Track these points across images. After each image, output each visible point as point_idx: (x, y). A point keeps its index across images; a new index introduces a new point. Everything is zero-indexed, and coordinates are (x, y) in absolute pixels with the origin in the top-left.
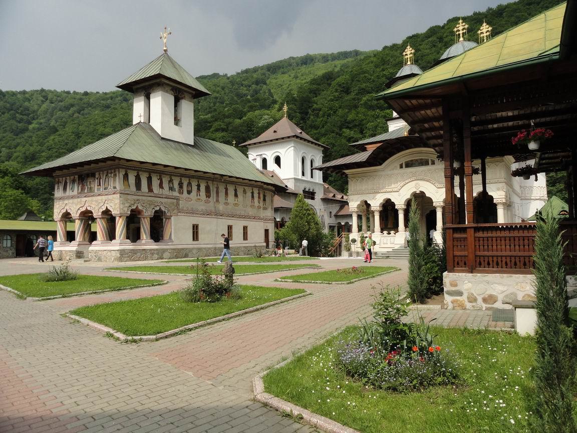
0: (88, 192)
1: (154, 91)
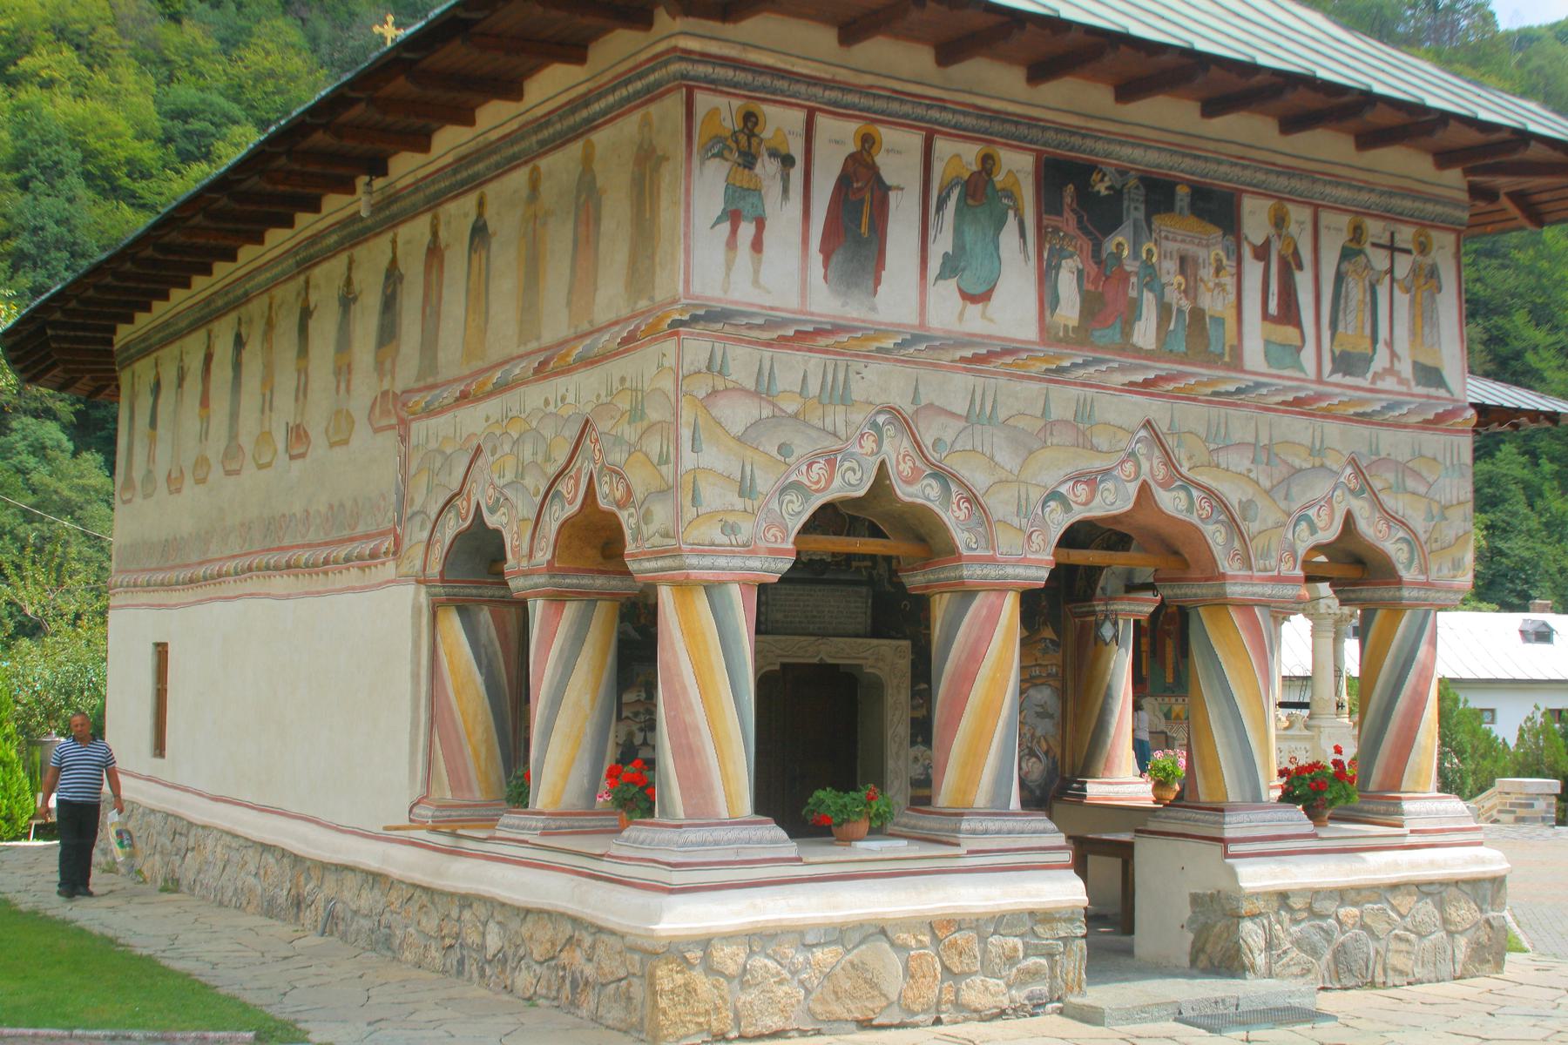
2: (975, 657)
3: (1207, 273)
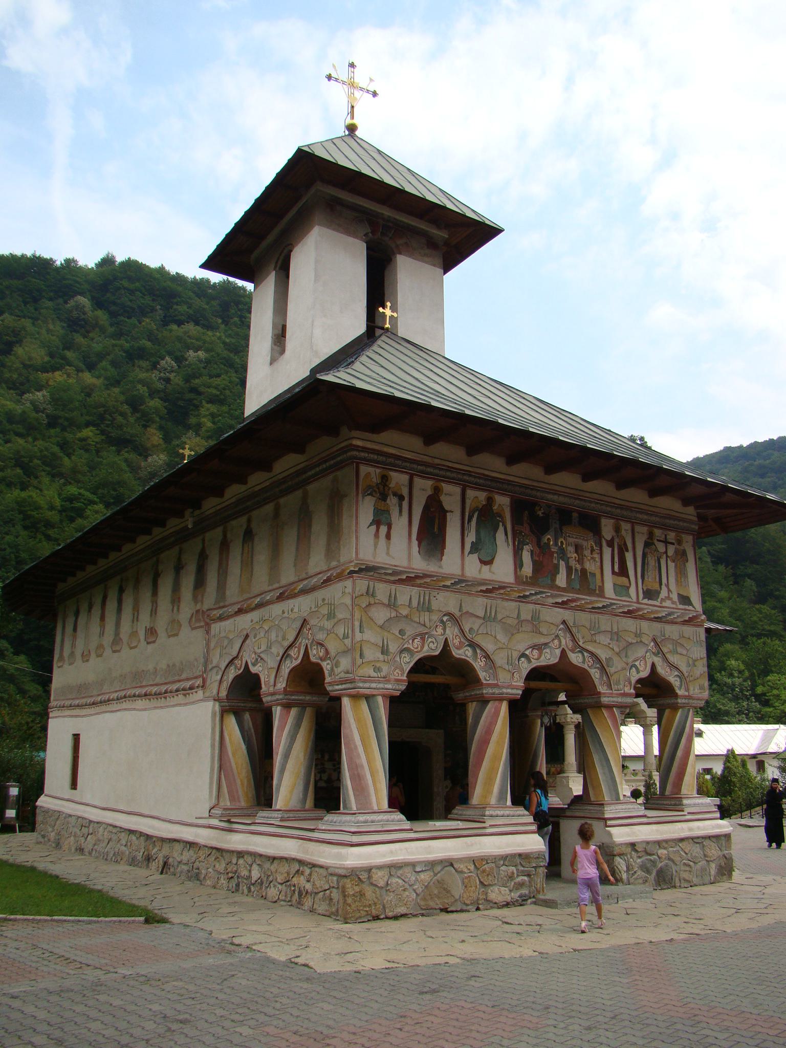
0: (569, 589)
1: (411, 252)
2: (489, 732)
3: (587, 553)
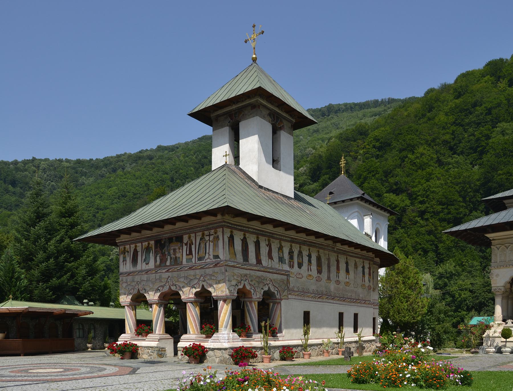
3: (177, 250)
